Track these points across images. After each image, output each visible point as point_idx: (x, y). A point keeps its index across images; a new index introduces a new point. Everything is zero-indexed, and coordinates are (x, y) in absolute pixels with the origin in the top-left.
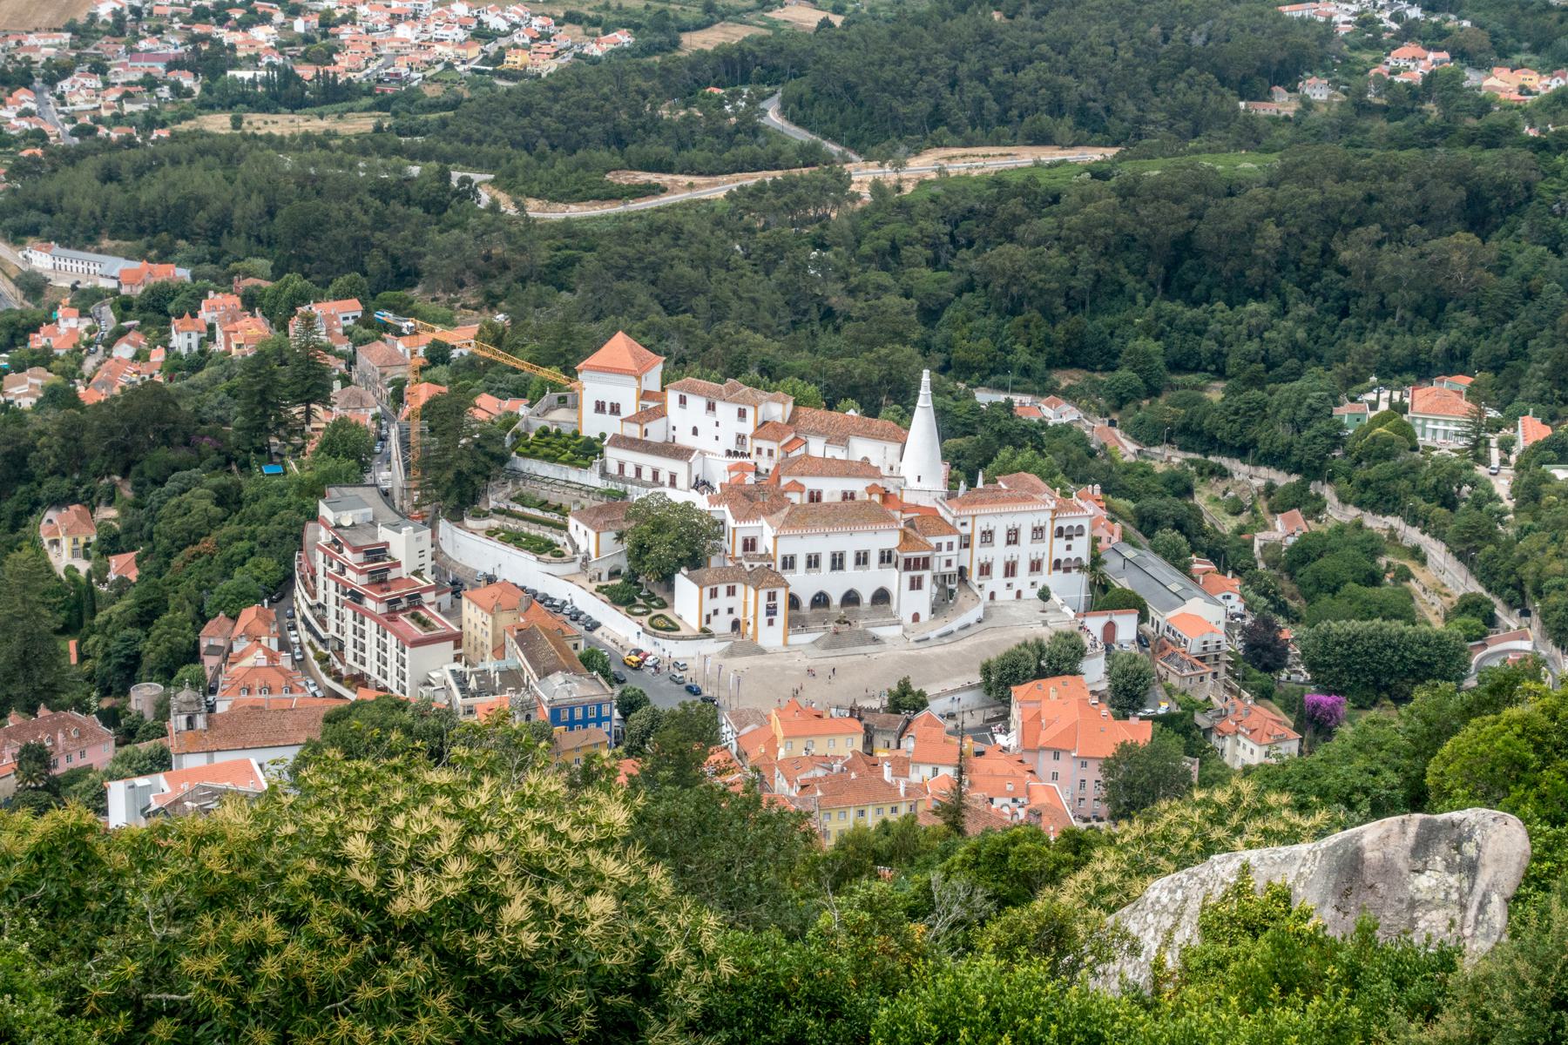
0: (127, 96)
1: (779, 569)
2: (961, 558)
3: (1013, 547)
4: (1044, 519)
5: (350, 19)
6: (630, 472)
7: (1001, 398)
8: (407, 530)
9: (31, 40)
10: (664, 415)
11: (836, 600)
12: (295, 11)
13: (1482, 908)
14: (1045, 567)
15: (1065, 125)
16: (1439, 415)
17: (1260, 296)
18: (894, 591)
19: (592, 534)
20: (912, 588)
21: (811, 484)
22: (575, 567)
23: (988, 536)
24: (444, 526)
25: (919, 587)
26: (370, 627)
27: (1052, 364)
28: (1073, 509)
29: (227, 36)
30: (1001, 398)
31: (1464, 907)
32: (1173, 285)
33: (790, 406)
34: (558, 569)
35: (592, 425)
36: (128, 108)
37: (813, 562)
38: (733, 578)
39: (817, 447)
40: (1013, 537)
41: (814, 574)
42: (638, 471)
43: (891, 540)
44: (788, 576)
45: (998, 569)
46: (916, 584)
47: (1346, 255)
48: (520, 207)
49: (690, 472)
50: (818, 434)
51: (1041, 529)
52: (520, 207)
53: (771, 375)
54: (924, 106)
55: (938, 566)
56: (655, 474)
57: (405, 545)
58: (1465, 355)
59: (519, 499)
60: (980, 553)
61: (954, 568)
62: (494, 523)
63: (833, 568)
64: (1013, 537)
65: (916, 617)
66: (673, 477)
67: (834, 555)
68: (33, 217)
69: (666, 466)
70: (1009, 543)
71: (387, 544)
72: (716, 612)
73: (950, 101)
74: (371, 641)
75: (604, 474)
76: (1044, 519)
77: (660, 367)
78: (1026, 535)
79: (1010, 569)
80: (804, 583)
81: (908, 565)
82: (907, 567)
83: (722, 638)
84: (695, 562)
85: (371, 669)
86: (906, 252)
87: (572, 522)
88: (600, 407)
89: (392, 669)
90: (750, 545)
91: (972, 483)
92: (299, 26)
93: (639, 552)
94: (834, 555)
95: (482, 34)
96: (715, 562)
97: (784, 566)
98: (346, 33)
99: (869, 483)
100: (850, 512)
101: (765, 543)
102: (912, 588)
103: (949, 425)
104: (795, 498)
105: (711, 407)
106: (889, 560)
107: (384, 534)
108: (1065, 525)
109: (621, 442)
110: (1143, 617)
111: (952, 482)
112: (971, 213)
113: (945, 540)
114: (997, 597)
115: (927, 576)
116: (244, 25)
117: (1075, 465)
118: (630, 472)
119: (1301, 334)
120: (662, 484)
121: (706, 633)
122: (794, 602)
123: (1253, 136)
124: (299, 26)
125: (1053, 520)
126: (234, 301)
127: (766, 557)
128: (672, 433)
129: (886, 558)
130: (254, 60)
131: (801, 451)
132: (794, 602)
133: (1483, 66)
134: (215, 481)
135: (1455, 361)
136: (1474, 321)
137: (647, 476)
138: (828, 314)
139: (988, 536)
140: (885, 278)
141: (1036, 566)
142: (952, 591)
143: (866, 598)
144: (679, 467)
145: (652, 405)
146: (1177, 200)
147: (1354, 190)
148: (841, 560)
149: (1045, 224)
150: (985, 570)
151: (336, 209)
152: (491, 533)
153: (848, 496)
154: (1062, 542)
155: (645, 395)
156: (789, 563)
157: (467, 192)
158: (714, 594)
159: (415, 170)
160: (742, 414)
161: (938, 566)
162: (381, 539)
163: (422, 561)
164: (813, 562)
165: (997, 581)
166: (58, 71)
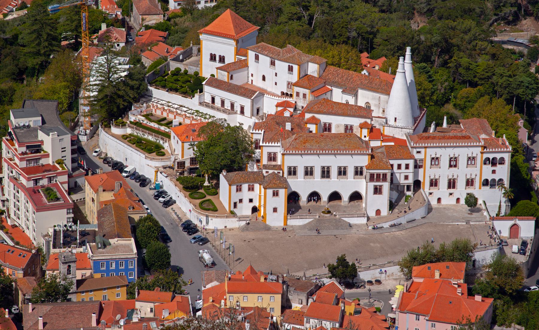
1: (286, 175)
3: (453, 169)
6: (218, 103)
10: (247, 66)
11: (325, 198)
14: (477, 183)
18: (363, 194)
19: (180, 142)
21: (324, 119)
23: (435, 160)
26: (22, 196)
28: (498, 147)
35: (208, 69)
37: (309, 172)
39: (338, 96)
40: (453, 163)
41: (309, 179)
42: (223, 103)
43: (363, 161)
45: (443, 183)
46: (377, 191)
49: (252, 106)
50: (338, 85)
56: (232, 105)
61: (411, 181)
63: (323, 176)
64: (453, 163)
65: (378, 212)
66: (242, 109)
67: (323, 168)
69: (240, 101)
70: (451, 166)
71: (42, 142)
72: (241, 201)
78: (462, 162)
79: (452, 184)
80: (302, 186)
81: (372, 178)
87: (173, 134)
88: (213, 58)
90: (272, 157)
91: (439, 124)
94: (323, 168)
96: (252, 168)
97: (290, 173)
99: (362, 120)
101: (279, 157)
104: (313, 128)
105: (273, 63)
106: (361, 173)
108: (491, 156)
109: (214, 82)
113: (403, 163)
114: (443, 202)
120: (236, 113)
122: (293, 198)
125: (482, 153)
127: (280, 167)
128: (250, 78)
129: (359, 172)
137: (228, 106)
139: (435, 160)
141: (470, 183)
143: (345, 197)
145: (243, 58)
148: (328, 172)
150: (434, 183)
152: (125, 138)
153: (349, 129)
156: (293, 172)
158: (239, 189)
160: (290, 69)
162: (40, 139)
163: (64, 154)
164: (309, 172)
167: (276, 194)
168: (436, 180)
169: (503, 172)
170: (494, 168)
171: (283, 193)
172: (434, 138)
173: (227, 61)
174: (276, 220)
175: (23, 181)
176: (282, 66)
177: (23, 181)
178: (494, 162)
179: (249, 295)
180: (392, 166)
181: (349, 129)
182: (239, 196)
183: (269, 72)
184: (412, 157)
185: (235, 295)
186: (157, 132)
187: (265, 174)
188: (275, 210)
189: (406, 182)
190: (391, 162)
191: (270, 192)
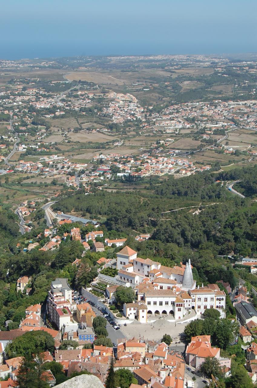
2: (193, 304)
9: (78, 166)
11: (161, 312)
20: (178, 311)
23: (200, 299)
25: (180, 311)
33: (160, 266)
37: (155, 303)
40: (206, 300)
46: (179, 310)
51: (213, 298)
55: (186, 305)
61: (191, 306)
63: (160, 305)
64: (206, 300)
65: (180, 318)
72: (131, 314)
77: (136, 254)
78: (209, 300)
82: (177, 306)
91: (201, 286)
94: (160, 302)
97: (148, 304)
99: (173, 285)
102: (178, 311)
108: (219, 297)
115: (182, 308)
122: (150, 312)
129: (173, 303)
130: (124, 171)
131: (161, 276)
139: (199, 299)
142: (190, 312)
148: (162, 303)
150: (199, 307)
153: (169, 288)
154: (218, 302)
156: (149, 303)
161: (186, 305)
163: (69, 297)
164: (155, 303)
167: (143, 311)
168: (200, 306)
169: (223, 303)
170: (220, 302)
171: (146, 311)
172: (199, 291)
178: (219, 300)
179: (134, 348)
180: (184, 301)
181: (169, 288)
184: (191, 298)
185: (129, 348)
187: (139, 304)
188: (143, 317)
189: (189, 307)
190: (184, 300)
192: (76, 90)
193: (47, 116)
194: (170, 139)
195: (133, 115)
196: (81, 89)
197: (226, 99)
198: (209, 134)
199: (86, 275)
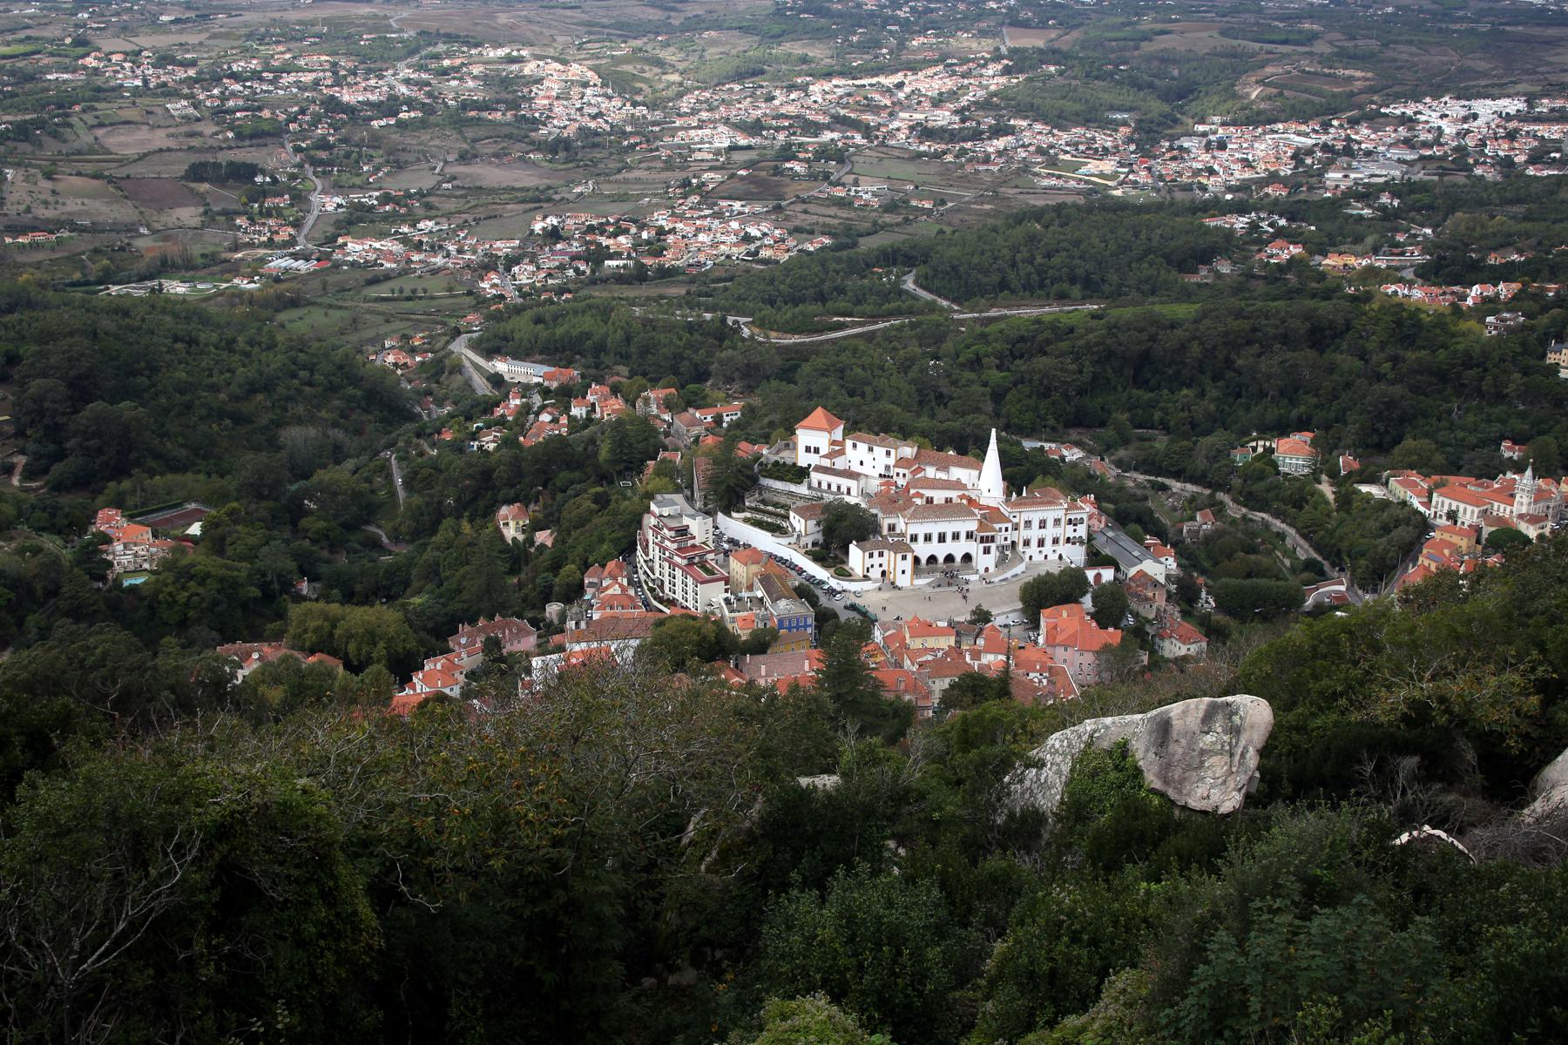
0: (550, 275)
2: (1013, 536)
4: (1060, 514)
5: (673, 231)
6: (824, 486)
7: (1039, 444)
8: (699, 519)
9: (498, 244)
12: (642, 227)
13: (1243, 755)
14: (1061, 541)
15: (1076, 291)
16: (1293, 454)
17: (1189, 386)
18: (974, 555)
21: (928, 493)
22: (793, 540)
23: (1028, 524)
24: (720, 515)
26: (678, 572)
27: (1067, 426)
29: (605, 241)
30: (1039, 444)
31: (1232, 755)
32: (1138, 381)
34: (785, 541)
35: (803, 460)
36: (550, 281)
38: (884, 546)
39: (931, 472)
40: (1043, 524)
41: (928, 545)
43: (972, 526)
44: (913, 546)
45: (1034, 543)
46: (987, 551)
47: (1240, 362)
48: (767, 337)
50: (932, 465)
52: (767, 337)
53: (905, 434)
54: (996, 278)
57: (699, 527)
58: (1309, 420)
59: (763, 502)
60: (1024, 533)
62: (748, 515)
64: (1043, 524)
65: (987, 570)
68: (497, 343)
69: (845, 483)
73: (1011, 275)
74: (678, 581)
75: (810, 487)
76: (1060, 514)
78: (1050, 523)
79: (1041, 543)
83: (876, 581)
84: (861, 539)
85: (679, 596)
86: (985, 360)
87: (792, 514)
88: (808, 449)
89: (690, 596)
90: (892, 528)
91: (1019, 493)
92: (645, 235)
93: (829, 531)
95: (747, 239)
98: (671, 239)
100: (949, 509)
101: (901, 525)
103: (1008, 462)
104: (918, 501)
105: (871, 449)
107: (686, 521)
109: (819, 469)
110: (1118, 569)
111: (1008, 494)
112: (1022, 339)
113: (1003, 526)
115: (993, 546)
116: (615, 235)
117: (1077, 484)
118: (824, 486)
119: (1212, 407)
121: (866, 578)
122: (917, 560)
123: (1187, 295)
124: (645, 235)
126: (606, 390)
127: (903, 535)
129: (970, 536)
130: (617, 255)
132: (917, 560)
133: (1325, 254)
134: (593, 491)
135: (1302, 425)
136: (1313, 400)
137: (834, 488)
138: (940, 397)
139: (1028, 524)
140: (972, 376)
141: (1056, 541)
143: (958, 558)
144: (852, 484)
146: (1141, 331)
147: (1245, 325)
149: (1064, 345)
150: (1027, 543)
151: (662, 338)
152: (746, 520)
153: (949, 501)
154: (1071, 527)
155: (834, 443)
156: (914, 538)
157: (737, 330)
158: (871, 556)
159: (708, 316)
160: (888, 453)
164: (928, 538)
165: (1033, 549)
166: (512, 261)
167: (904, 558)
171: (910, 557)
173: (822, 452)
174: (904, 581)
175: (677, 559)
176: (879, 451)
177: (677, 559)
182: (872, 561)
183: (867, 457)
186: (777, 515)
191: (899, 556)
192: (437, 57)
193: (375, 123)
194: (712, 175)
195: (600, 115)
196: (449, 55)
197: (828, 75)
198: (807, 161)
199: (732, 482)
